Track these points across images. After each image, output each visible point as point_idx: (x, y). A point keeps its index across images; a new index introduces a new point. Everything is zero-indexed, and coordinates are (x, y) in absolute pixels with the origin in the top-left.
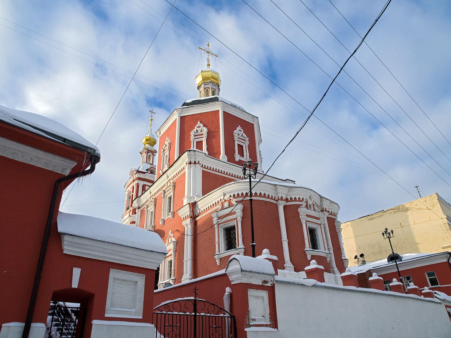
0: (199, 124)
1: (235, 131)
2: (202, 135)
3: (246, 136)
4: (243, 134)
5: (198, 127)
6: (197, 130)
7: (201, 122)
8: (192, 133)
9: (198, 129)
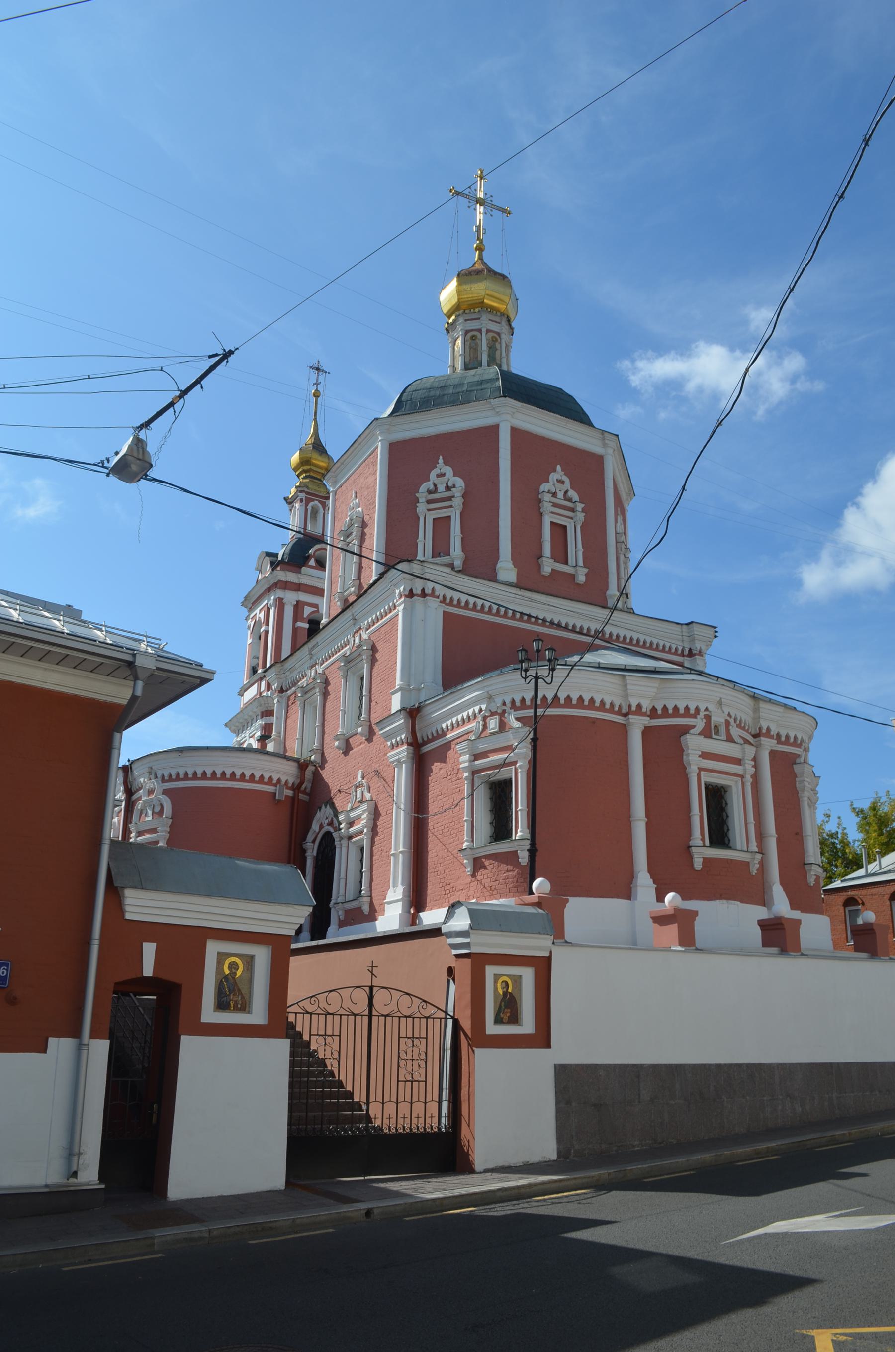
0: (441, 466)
1: (544, 487)
5: (438, 476)
6: (435, 485)
7: (446, 463)
9: (438, 481)
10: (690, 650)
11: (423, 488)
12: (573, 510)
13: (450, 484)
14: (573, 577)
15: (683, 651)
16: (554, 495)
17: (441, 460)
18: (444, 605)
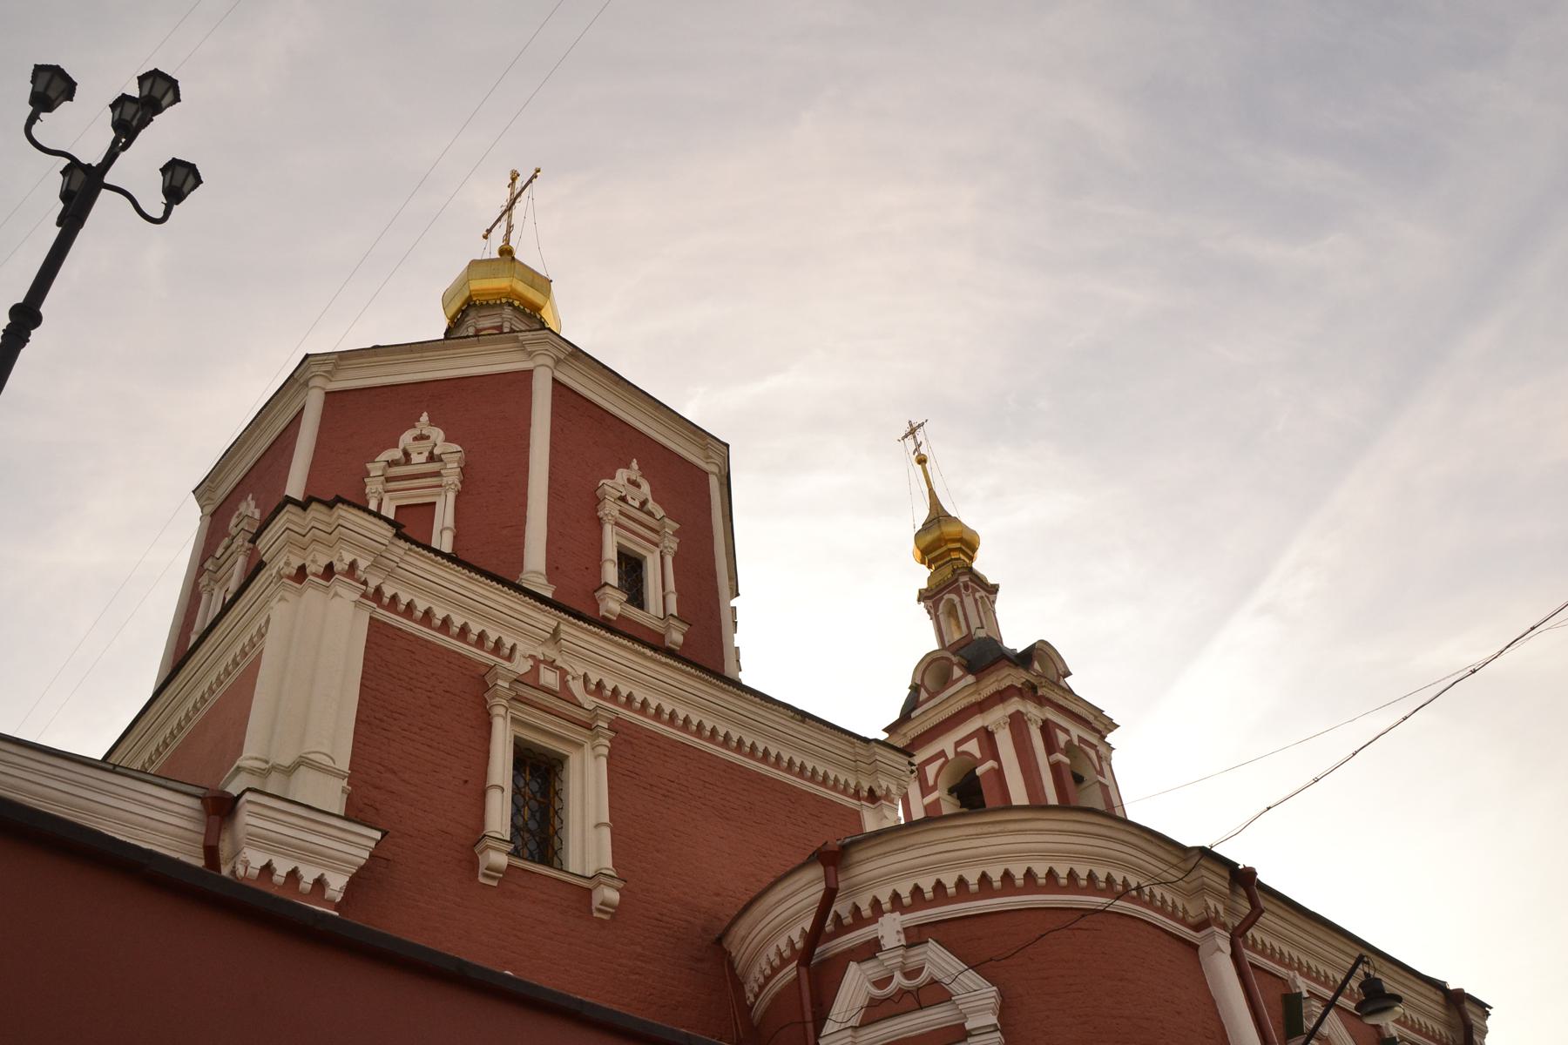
2: (437, 474)
3: (659, 512)
6: (406, 454)
7: (433, 422)
8: (376, 468)
10: (871, 790)
13: (436, 451)
18: (375, 605)
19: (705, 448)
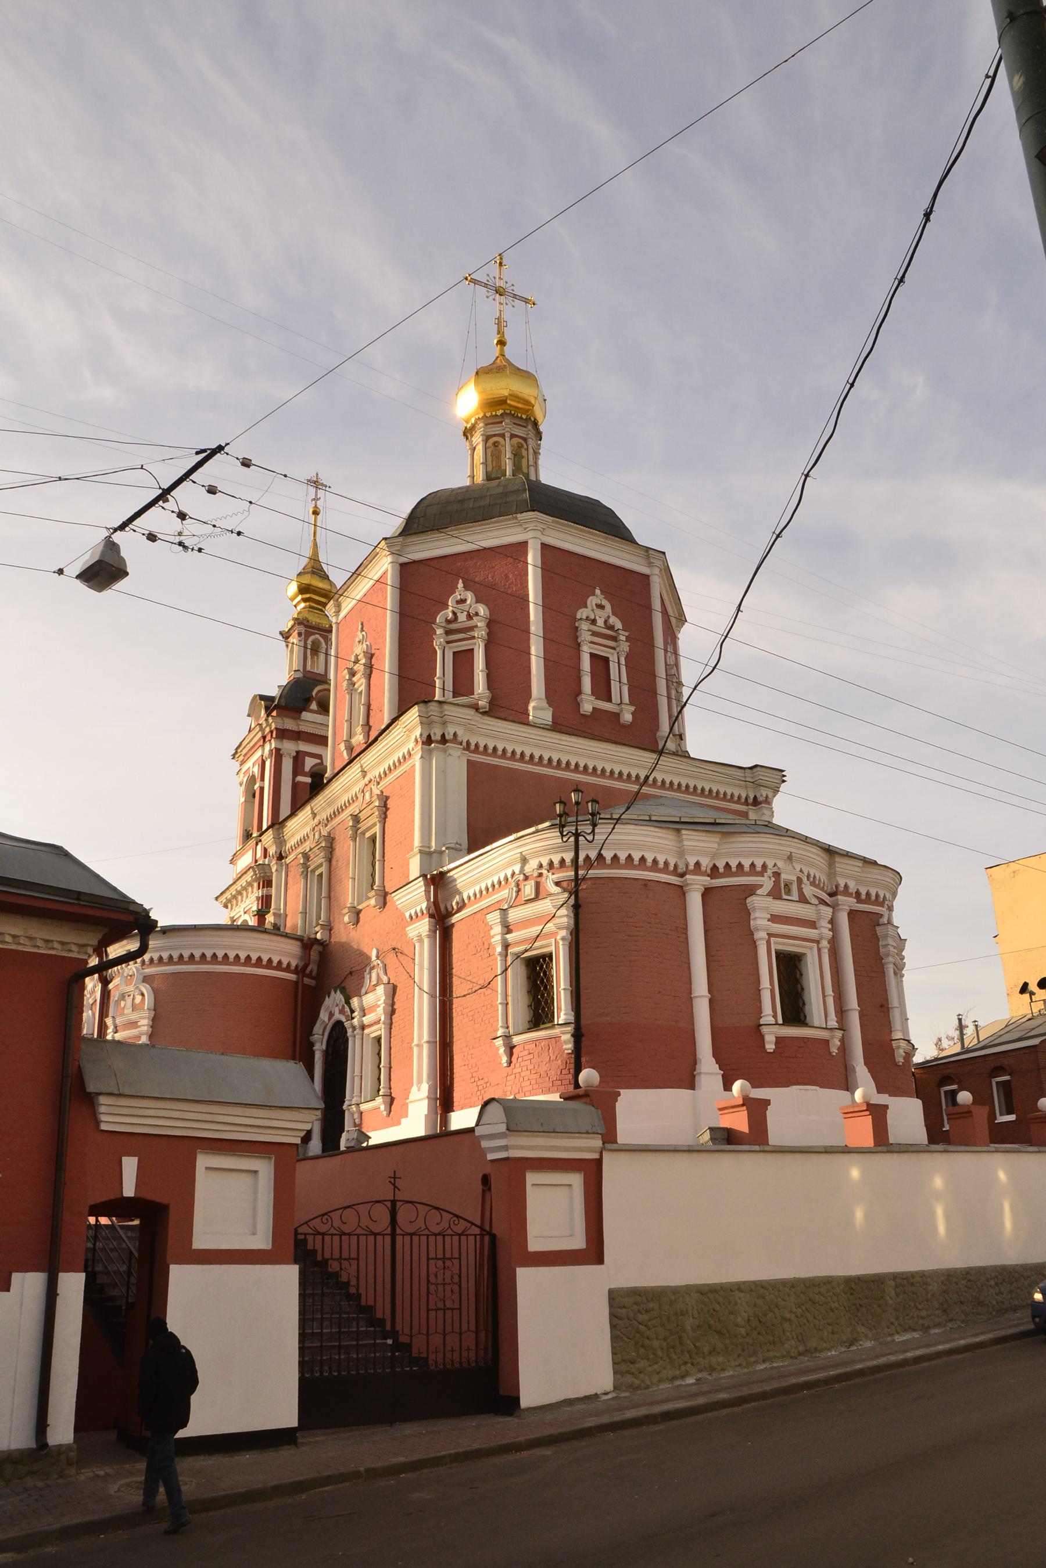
1: (582, 613)
3: (619, 625)
4: (609, 617)
6: (454, 613)
10: (755, 798)
11: (439, 619)
12: (615, 639)
14: (617, 716)
15: (746, 799)
16: (594, 622)
17: (460, 585)
18: (467, 752)
19: (648, 557)
